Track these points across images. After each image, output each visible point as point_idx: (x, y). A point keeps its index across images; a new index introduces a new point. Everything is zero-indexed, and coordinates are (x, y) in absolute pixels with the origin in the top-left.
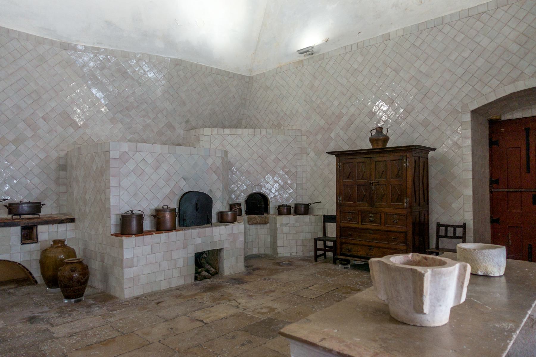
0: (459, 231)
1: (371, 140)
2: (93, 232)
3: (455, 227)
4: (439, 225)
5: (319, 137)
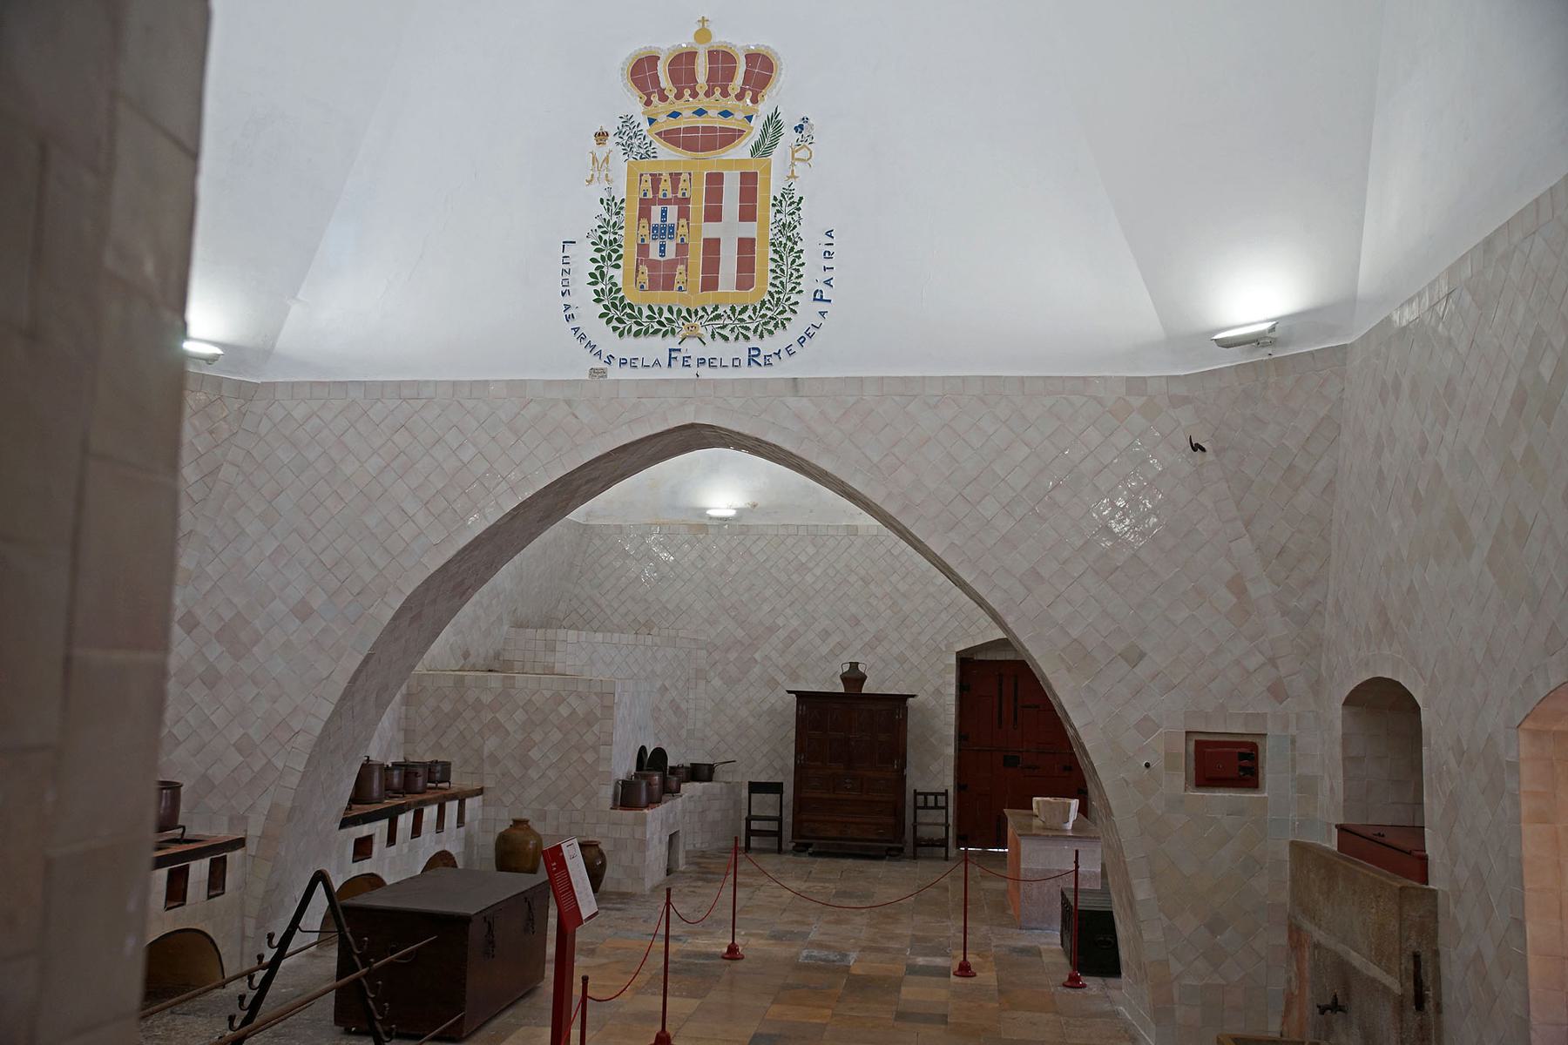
0: (941, 799)
1: (844, 678)
2: (552, 807)
3: (936, 795)
4: (916, 793)
5: (732, 656)
